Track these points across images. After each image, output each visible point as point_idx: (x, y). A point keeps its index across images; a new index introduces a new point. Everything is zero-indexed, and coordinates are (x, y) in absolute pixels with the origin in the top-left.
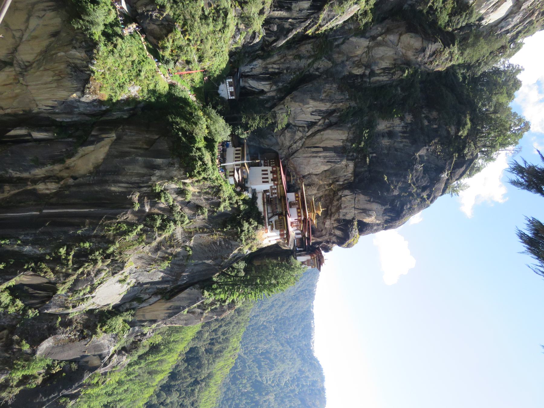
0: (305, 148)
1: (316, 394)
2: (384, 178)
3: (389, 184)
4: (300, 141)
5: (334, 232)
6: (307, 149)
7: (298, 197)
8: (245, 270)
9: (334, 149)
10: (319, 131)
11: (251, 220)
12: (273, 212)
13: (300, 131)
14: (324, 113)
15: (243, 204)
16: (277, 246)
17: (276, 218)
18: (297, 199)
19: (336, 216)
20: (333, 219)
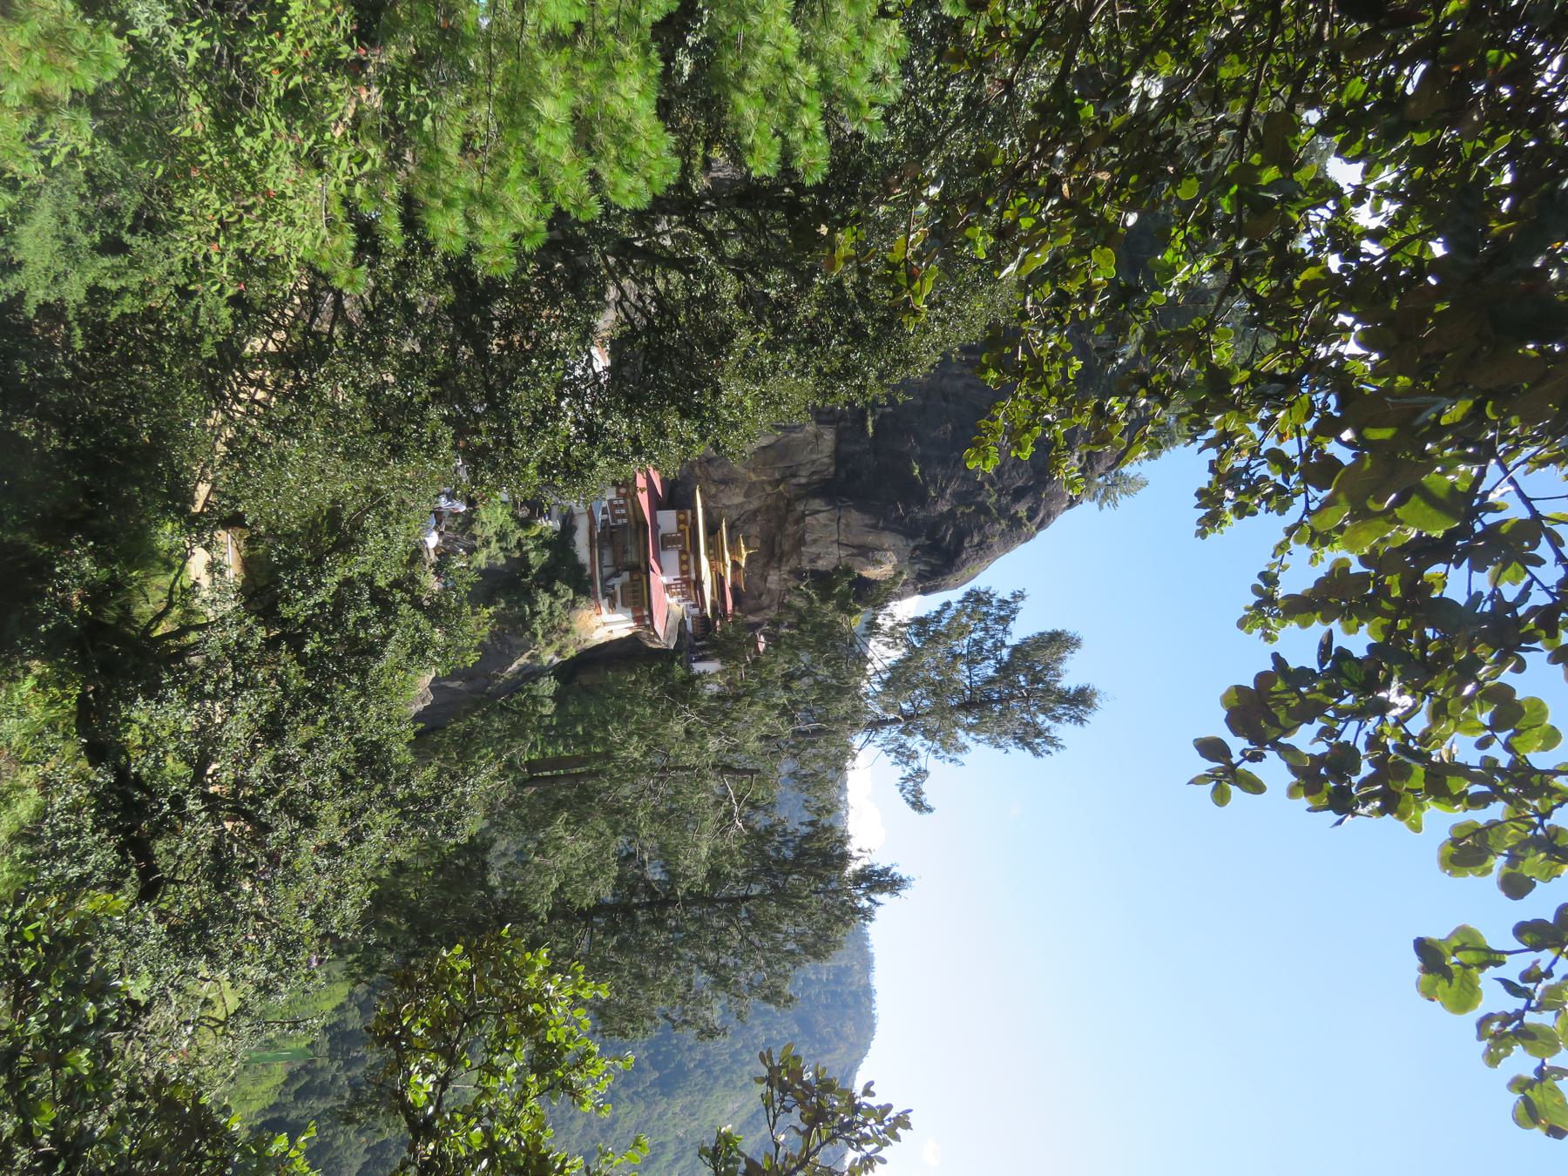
1: (845, 1006)
2: (911, 470)
3: (925, 486)
7: (684, 522)
8: (558, 697)
11: (558, 585)
12: (615, 563)
15: (536, 548)
16: (634, 638)
17: (626, 576)
19: (793, 563)
20: (786, 568)
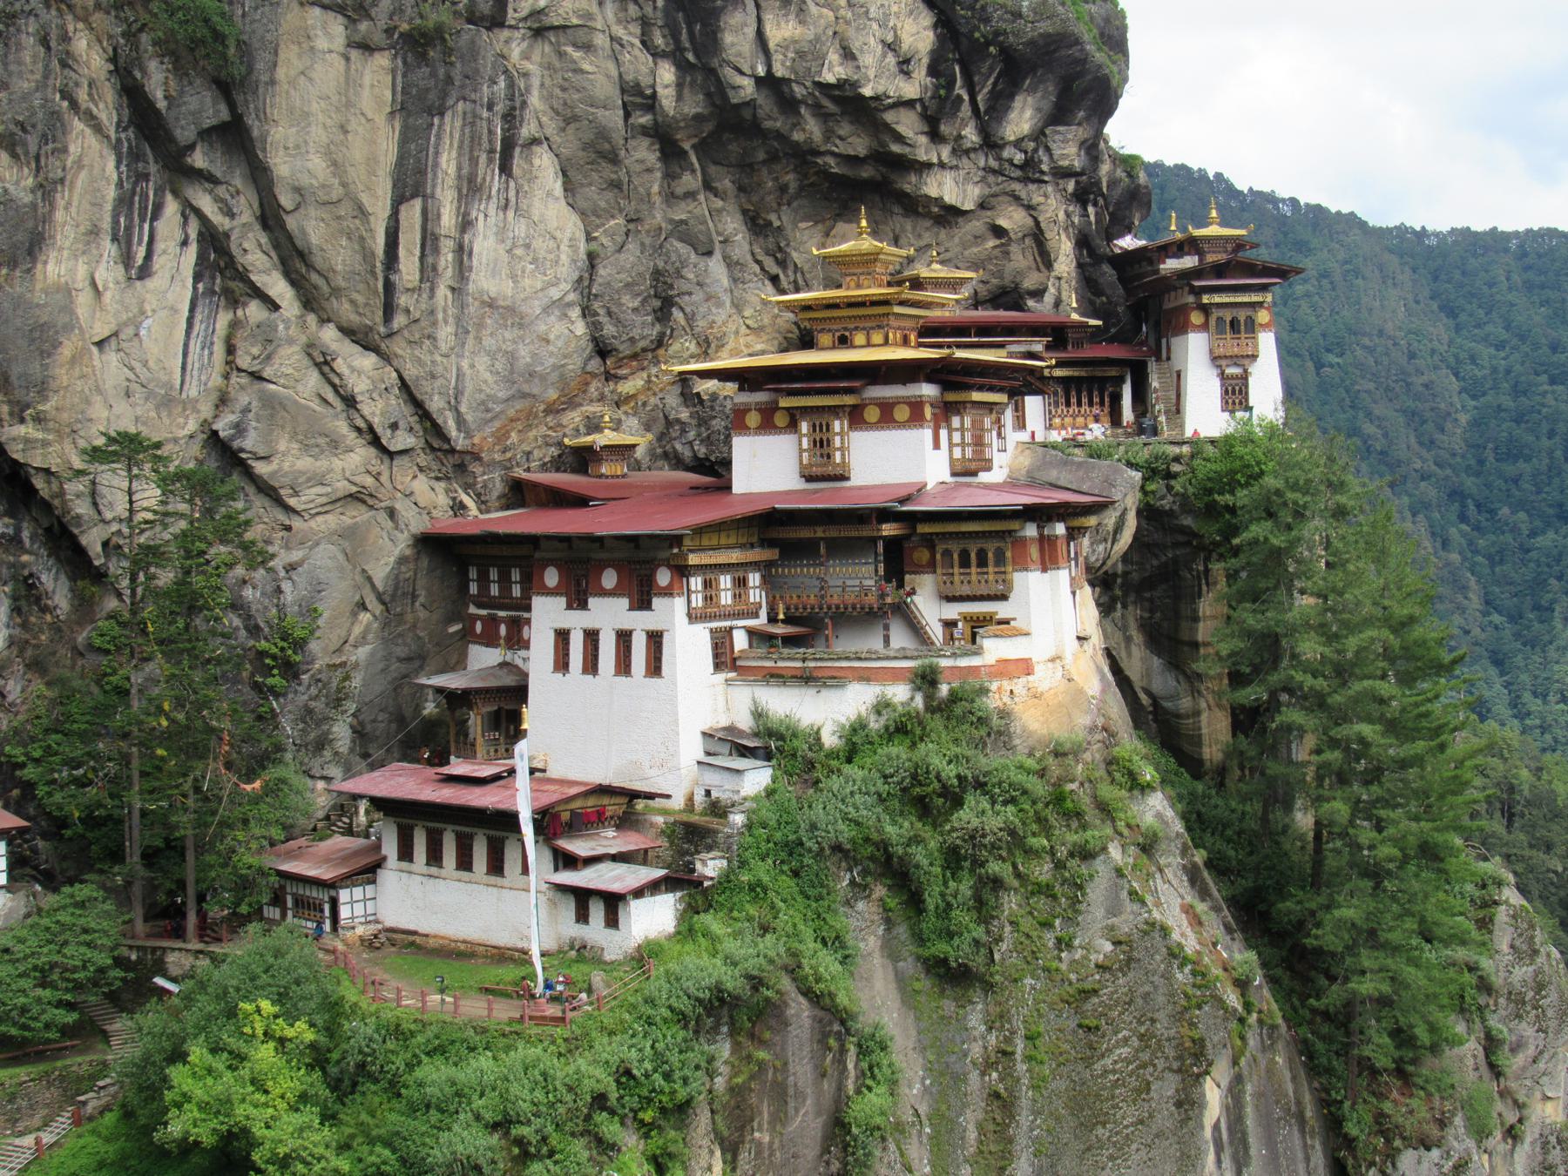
0: (390, 335)
4: (339, 365)
5: (1018, 144)
6: (399, 320)
9: (417, 110)
10: (270, 218)
13: (269, 357)
14: (146, 177)
16: (1108, 587)
18: (780, 419)
19: (908, 124)
20: (924, 150)
